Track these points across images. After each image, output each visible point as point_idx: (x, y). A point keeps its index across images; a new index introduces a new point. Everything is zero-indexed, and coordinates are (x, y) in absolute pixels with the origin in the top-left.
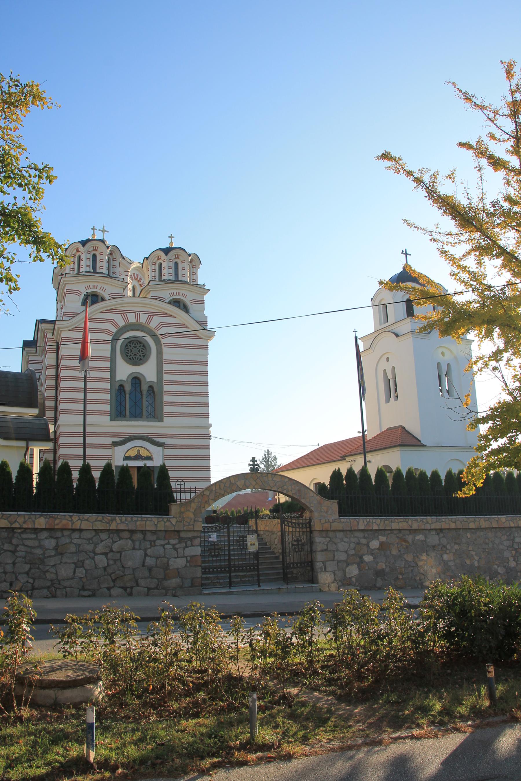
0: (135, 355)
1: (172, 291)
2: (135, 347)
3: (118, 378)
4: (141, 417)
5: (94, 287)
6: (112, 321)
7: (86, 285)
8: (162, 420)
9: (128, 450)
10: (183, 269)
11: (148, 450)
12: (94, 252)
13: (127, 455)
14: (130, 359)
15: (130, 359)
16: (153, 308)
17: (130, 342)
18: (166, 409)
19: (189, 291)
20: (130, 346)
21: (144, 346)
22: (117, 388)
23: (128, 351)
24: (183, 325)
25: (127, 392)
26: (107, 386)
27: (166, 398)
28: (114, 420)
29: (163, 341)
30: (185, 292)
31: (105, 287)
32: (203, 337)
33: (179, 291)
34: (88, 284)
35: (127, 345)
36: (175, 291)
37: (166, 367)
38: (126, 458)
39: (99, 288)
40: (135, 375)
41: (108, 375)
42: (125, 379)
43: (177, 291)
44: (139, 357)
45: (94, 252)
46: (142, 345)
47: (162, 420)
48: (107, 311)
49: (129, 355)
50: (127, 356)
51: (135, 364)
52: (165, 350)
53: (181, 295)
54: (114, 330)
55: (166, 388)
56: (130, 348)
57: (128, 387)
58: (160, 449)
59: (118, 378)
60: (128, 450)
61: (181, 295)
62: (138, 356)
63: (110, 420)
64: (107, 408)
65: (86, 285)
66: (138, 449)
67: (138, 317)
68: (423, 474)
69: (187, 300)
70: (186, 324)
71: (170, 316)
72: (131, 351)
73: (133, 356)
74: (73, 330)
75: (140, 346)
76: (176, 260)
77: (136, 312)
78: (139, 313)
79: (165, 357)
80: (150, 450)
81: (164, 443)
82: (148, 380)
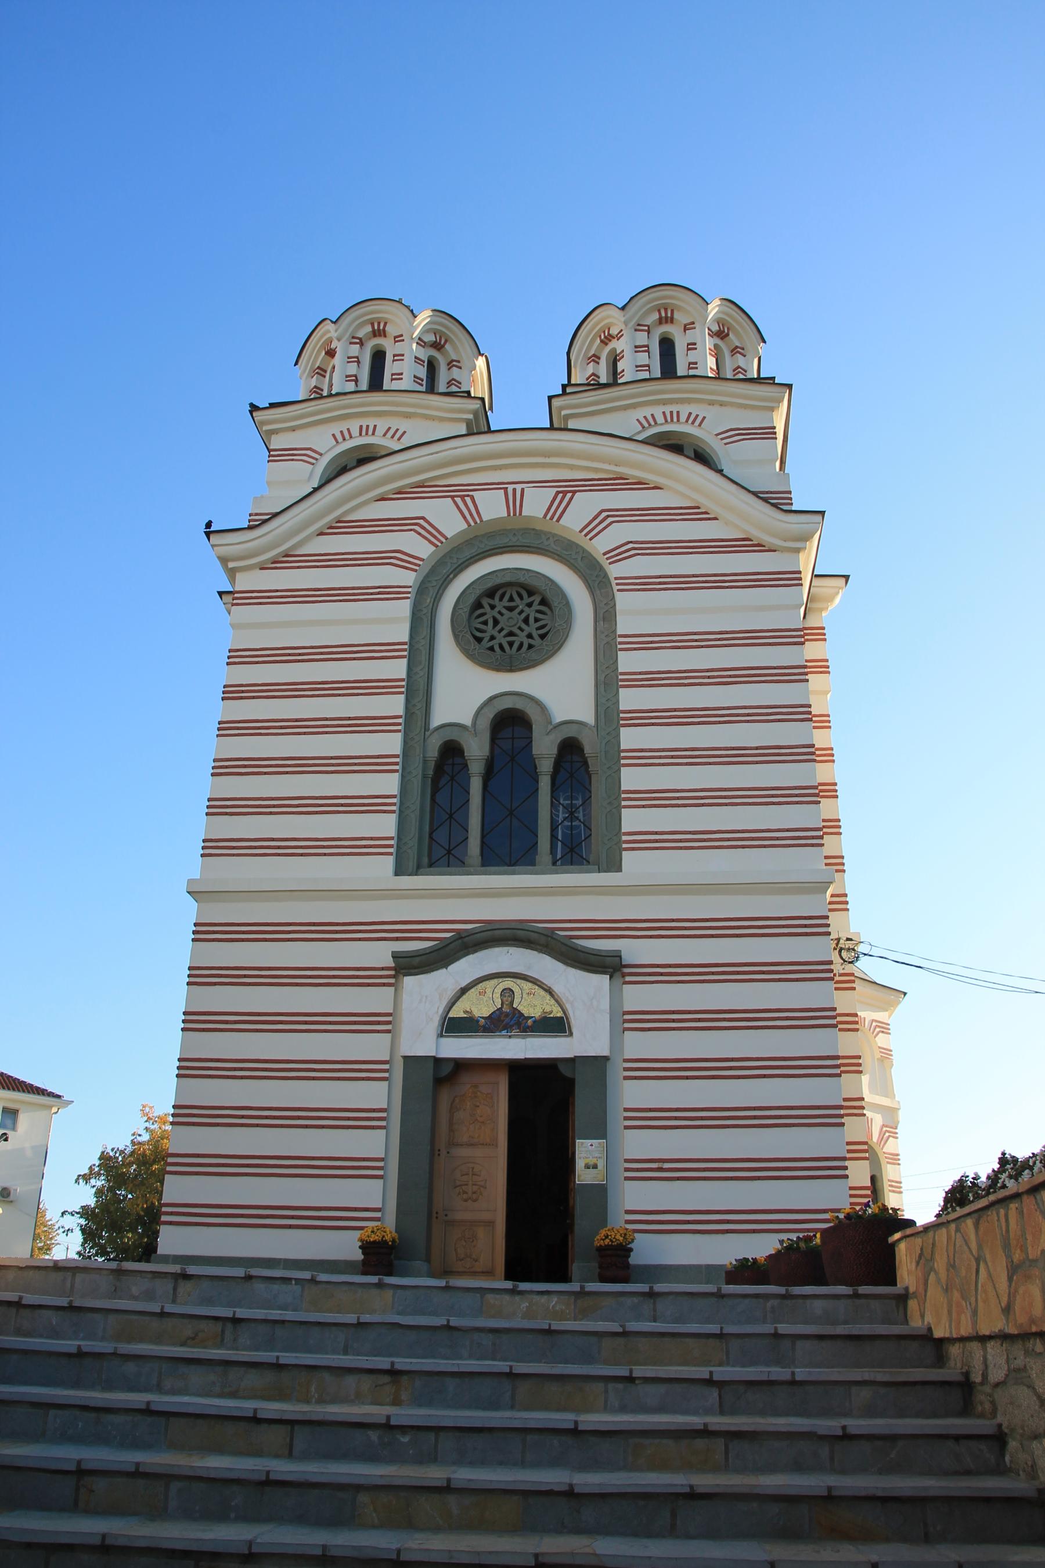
0: (511, 634)
1: (647, 412)
2: (511, 609)
3: (436, 721)
4: (533, 863)
7: (336, 428)
8: (615, 866)
9: (464, 991)
10: (691, 346)
11: (549, 991)
13: (457, 1012)
14: (492, 649)
15: (492, 649)
16: (572, 467)
17: (491, 593)
18: (632, 820)
19: (711, 403)
20: (493, 607)
21: (544, 602)
22: (433, 752)
23: (485, 623)
24: (696, 513)
25: (476, 769)
26: (392, 743)
27: (631, 778)
28: (416, 872)
29: (614, 571)
30: (695, 409)
31: (403, 425)
32: (778, 542)
33: (674, 408)
34: (343, 426)
35: (478, 605)
36: (658, 411)
37: (628, 662)
38: (453, 1026)
39: (380, 431)
41: (395, 705)
42: (467, 720)
43: (667, 409)
46: (537, 599)
47: (615, 866)
48: (401, 494)
49: (487, 636)
50: (479, 640)
51: (511, 666)
52: (623, 601)
53: (683, 418)
55: (630, 738)
56: (490, 614)
57: (477, 750)
58: (602, 981)
59: (437, 719)
60: (464, 991)
61: (683, 418)
62: (522, 637)
63: (398, 872)
64: (386, 825)
66: (508, 983)
67: (514, 502)
69: (706, 435)
70: (706, 504)
71: (640, 485)
72: (496, 622)
73: (501, 639)
74: (275, 564)
75: (530, 605)
76: (666, 328)
77: (510, 488)
78: (519, 487)
79: (624, 626)
80: (557, 989)
81: (617, 955)
82: (559, 715)
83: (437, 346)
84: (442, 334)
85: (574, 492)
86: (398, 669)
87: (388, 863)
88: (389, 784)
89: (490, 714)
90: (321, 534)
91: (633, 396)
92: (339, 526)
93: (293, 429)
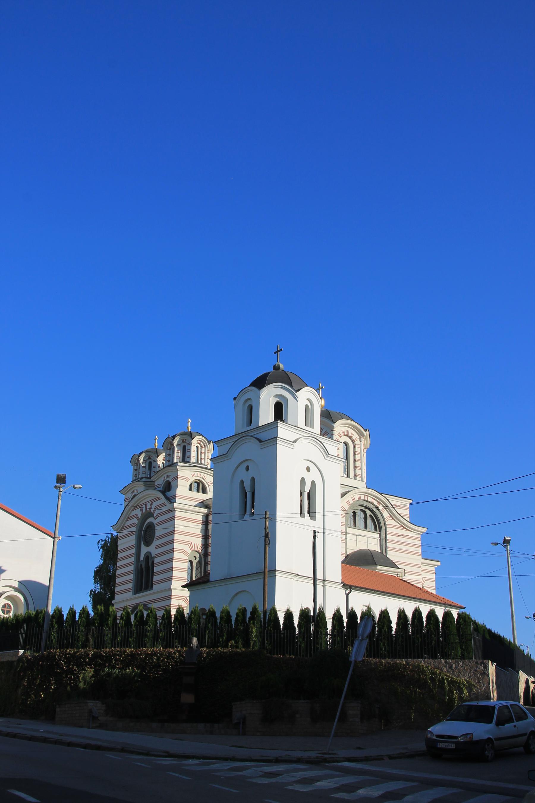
5: (134, 491)
6: (136, 516)
7: (130, 492)
12: (150, 460)
26: (132, 568)
30: (168, 474)
36: (165, 476)
40: (146, 555)
41: (132, 559)
44: (147, 538)
45: (150, 460)
54: (135, 521)
57: (143, 566)
64: (131, 585)
65: (130, 492)
68: (212, 614)
83: (150, 458)
84: (150, 456)
85: (153, 503)
86: (133, 551)
87: (130, 594)
88: (131, 577)
89: (145, 558)
90: (127, 521)
91: (161, 474)
92: (129, 518)
93: (126, 493)
